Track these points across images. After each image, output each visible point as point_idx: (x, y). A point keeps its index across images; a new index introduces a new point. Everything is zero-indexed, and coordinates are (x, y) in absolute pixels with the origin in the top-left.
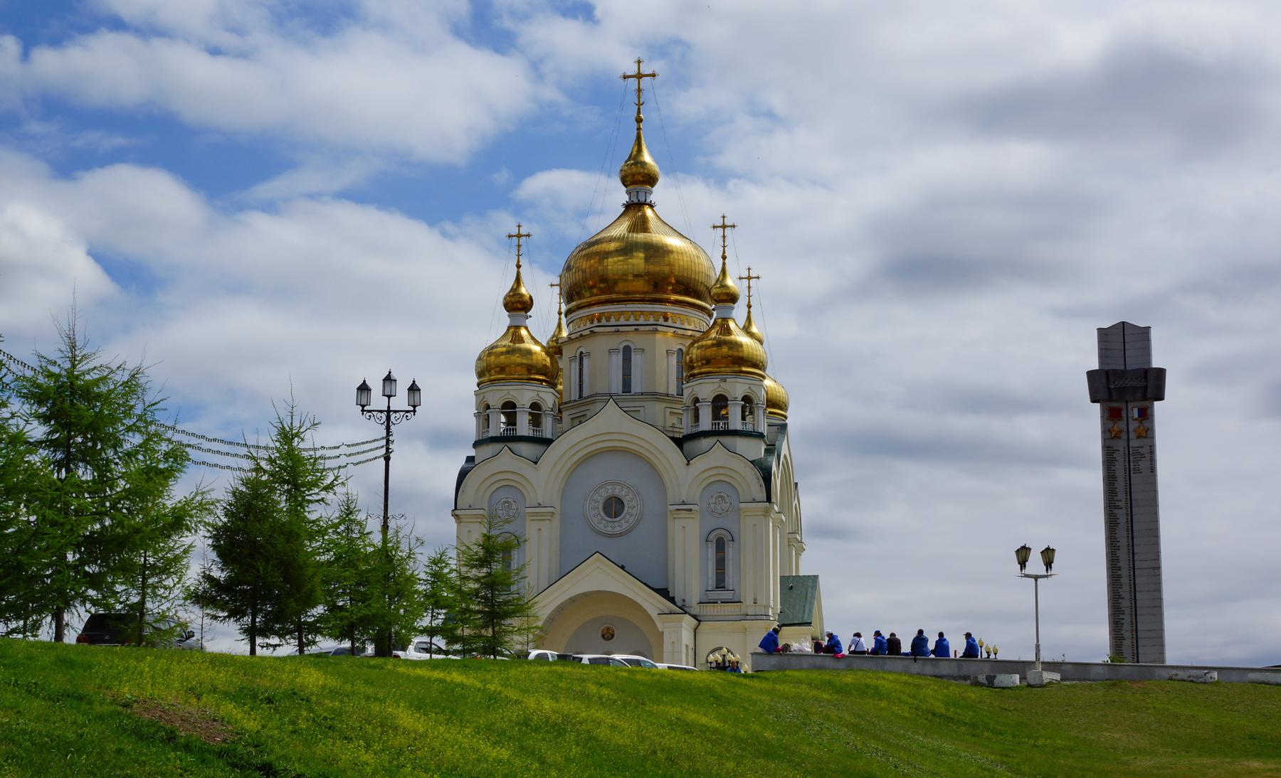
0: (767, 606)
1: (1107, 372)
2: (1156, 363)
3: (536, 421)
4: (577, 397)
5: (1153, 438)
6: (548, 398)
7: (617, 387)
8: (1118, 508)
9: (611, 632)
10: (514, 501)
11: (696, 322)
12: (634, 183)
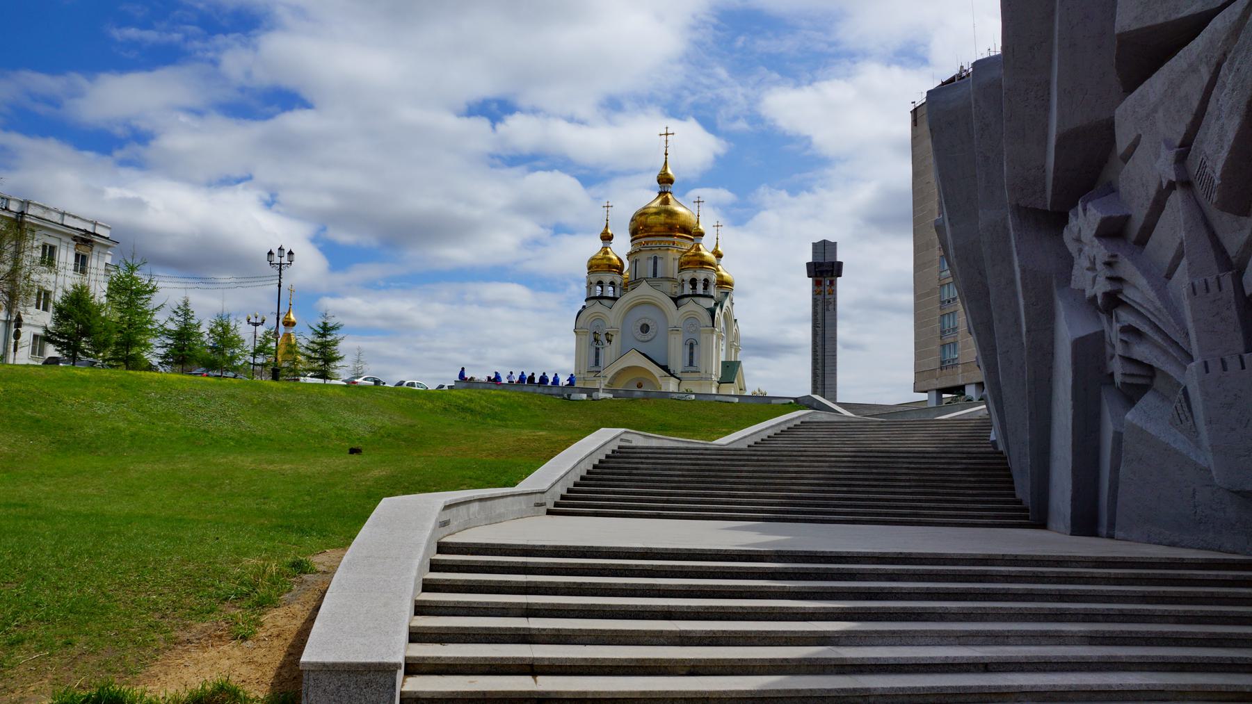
0: (711, 374)
1: (815, 263)
2: (839, 259)
5: (836, 294)
6: (618, 279)
7: (650, 274)
8: (818, 327)
11: (687, 245)
12: (663, 183)
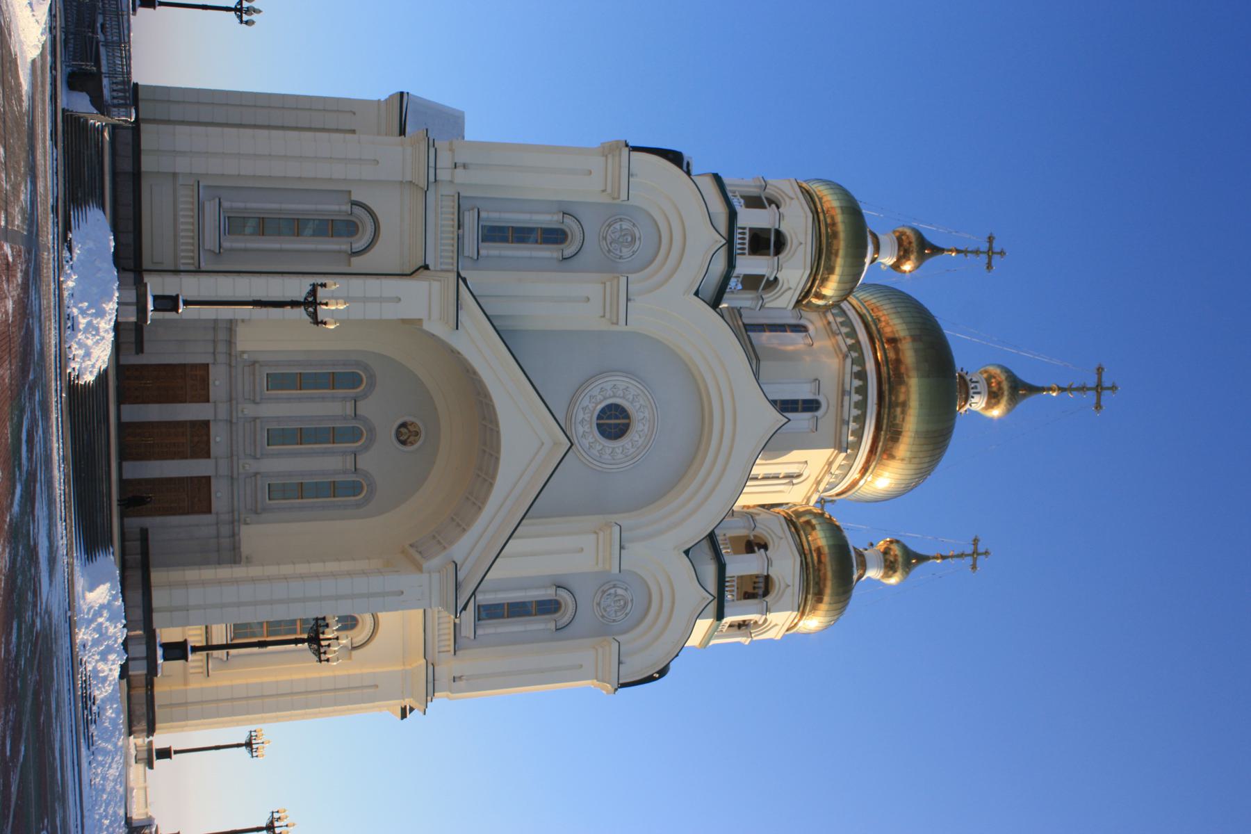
3: (752, 282)
4: (746, 321)
6: (781, 303)
9: (412, 439)
10: (634, 253)
